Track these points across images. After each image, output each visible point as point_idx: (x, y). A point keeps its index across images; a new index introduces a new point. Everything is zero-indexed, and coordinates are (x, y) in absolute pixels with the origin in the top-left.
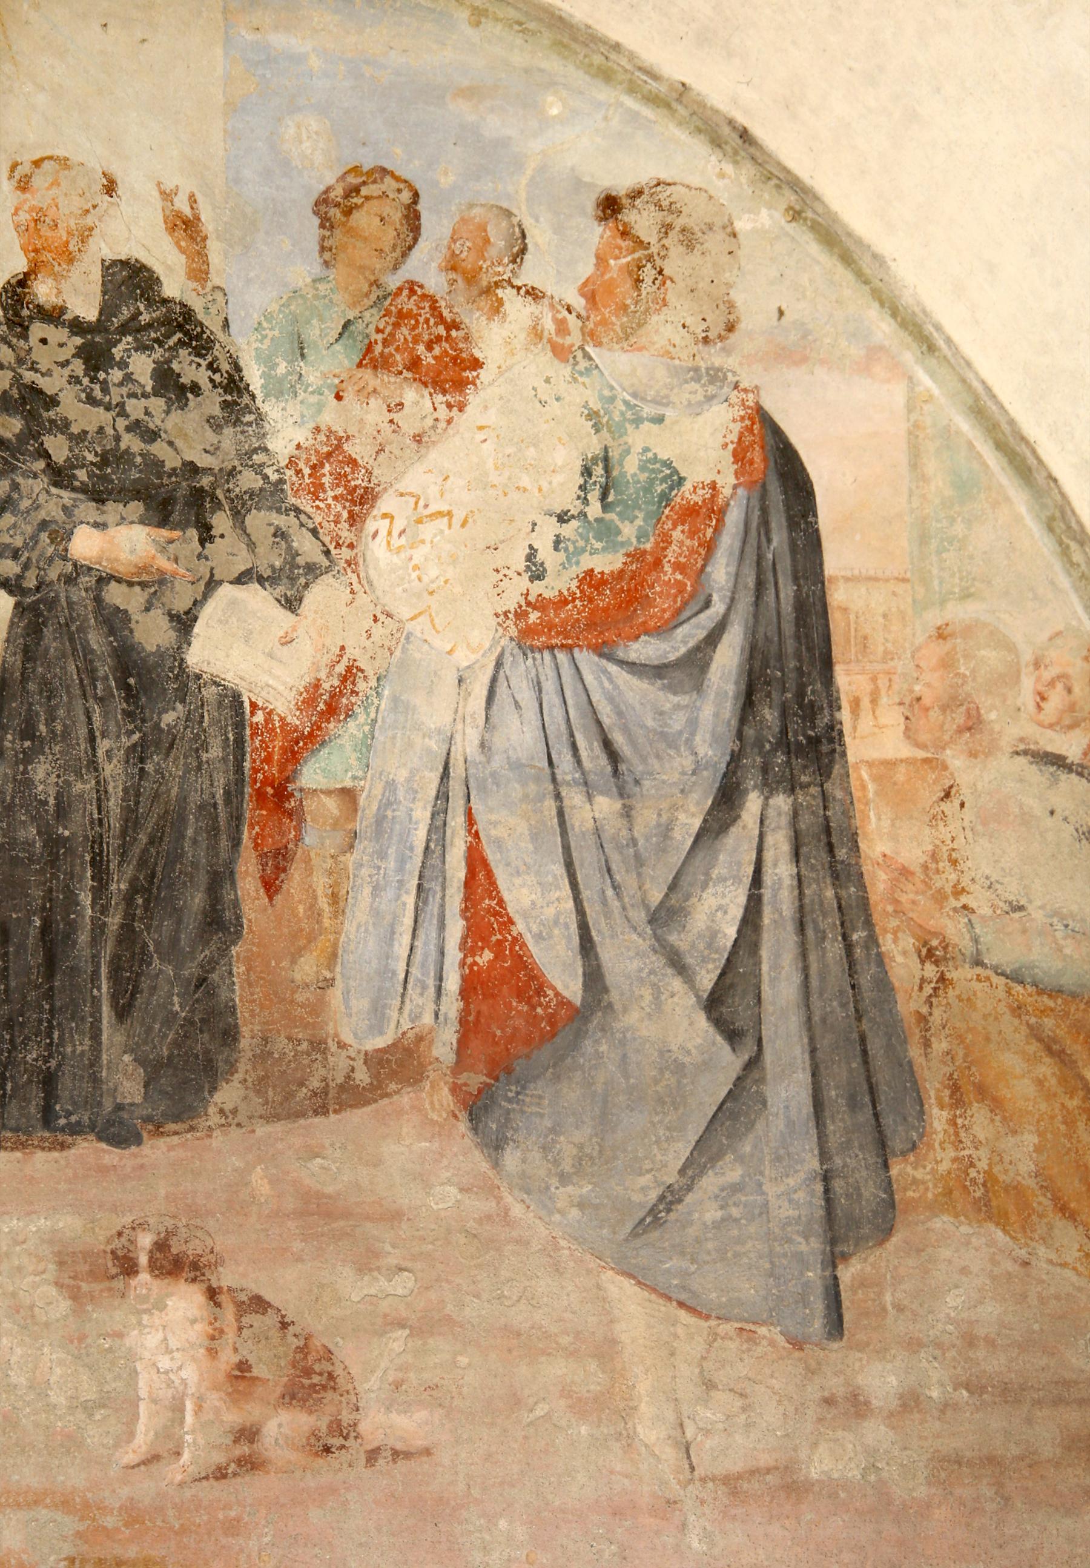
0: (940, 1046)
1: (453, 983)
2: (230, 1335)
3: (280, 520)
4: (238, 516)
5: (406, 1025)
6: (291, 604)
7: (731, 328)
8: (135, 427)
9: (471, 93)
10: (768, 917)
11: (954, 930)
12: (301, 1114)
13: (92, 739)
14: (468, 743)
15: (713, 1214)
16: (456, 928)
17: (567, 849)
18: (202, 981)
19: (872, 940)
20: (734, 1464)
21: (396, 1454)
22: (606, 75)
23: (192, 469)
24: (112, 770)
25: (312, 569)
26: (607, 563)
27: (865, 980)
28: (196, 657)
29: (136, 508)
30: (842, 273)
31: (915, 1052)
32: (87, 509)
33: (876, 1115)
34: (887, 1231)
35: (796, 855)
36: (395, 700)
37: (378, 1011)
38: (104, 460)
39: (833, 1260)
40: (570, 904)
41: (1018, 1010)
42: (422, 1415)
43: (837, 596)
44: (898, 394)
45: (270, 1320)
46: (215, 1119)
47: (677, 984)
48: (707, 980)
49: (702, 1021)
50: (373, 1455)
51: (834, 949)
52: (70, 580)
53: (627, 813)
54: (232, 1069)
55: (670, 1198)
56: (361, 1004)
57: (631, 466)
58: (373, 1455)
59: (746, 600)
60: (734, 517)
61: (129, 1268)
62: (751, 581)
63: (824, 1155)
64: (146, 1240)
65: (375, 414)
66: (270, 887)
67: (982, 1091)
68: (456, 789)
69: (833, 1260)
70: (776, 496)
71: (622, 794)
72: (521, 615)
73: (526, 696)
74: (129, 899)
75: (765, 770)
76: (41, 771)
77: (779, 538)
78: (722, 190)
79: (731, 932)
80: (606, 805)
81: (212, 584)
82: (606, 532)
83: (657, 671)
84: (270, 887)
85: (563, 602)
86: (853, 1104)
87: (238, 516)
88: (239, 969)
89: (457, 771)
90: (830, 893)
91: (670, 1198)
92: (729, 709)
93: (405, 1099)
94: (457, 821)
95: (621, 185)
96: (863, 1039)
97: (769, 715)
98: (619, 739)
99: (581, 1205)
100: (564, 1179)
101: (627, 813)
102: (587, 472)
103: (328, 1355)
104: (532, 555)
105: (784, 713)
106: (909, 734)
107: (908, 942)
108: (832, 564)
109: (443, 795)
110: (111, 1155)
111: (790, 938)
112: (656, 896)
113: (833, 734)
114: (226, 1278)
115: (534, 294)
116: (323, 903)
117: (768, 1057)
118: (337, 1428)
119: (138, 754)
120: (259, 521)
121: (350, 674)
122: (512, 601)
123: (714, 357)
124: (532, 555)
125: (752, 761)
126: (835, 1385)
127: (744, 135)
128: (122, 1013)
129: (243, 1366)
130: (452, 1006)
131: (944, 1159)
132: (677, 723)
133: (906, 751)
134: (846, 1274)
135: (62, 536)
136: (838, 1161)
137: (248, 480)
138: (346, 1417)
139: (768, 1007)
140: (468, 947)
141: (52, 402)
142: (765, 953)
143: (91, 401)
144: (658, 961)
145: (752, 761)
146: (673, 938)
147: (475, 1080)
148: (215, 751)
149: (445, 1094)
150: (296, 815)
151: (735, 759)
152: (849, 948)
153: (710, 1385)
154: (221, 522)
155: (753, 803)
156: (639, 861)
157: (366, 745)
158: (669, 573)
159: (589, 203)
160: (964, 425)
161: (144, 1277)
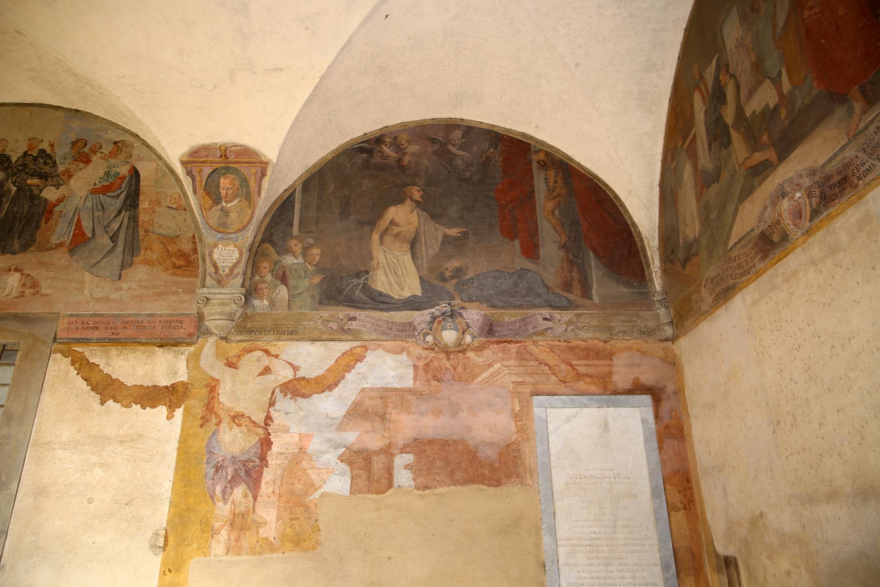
0: (145, 243)
1: (71, 235)
2: (24, 280)
3: (58, 179)
4: (52, 178)
5: (63, 240)
6: (57, 189)
7: (131, 156)
8: (39, 168)
9: (98, 130)
10: (122, 227)
11: (151, 229)
12: (43, 251)
13: (24, 205)
14: (81, 205)
15: (104, 264)
16: (73, 228)
17: (93, 219)
18: (32, 234)
19: (138, 230)
20: (99, 297)
21: (46, 295)
22: (118, 128)
23: (46, 173)
24: (26, 209)
25: (61, 185)
26: (106, 184)
27: (135, 235)
28: (42, 195)
29: (37, 177)
30: (149, 150)
31: (141, 244)
32: (30, 177)
33: (133, 252)
34: (131, 267)
35: (129, 219)
36: (71, 200)
37: (59, 238)
38: (34, 172)
39: (122, 270)
40: (92, 225)
41: (158, 238)
42: (50, 290)
43: (141, 188)
44: (155, 164)
45: (31, 277)
46: (29, 251)
47: (106, 235)
48: (111, 235)
49: (109, 240)
50: (42, 295)
51: (132, 231)
52: (25, 186)
53: (104, 214)
54: (34, 245)
55: (98, 262)
56: (56, 237)
57: (112, 172)
58: (42, 295)
59: (127, 189)
60: (127, 179)
61: (10, 270)
62: (128, 186)
63: (123, 257)
64: (14, 267)
65: (75, 166)
66: (46, 223)
67: (150, 249)
68: (77, 211)
69: (122, 270)
70: (134, 175)
71: (103, 211)
72: (92, 190)
73: (91, 200)
74: (24, 224)
75: (126, 209)
76: (15, 209)
77: (134, 181)
78: (132, 141)
79: (116, 229)
80: (100, 213)
81: (46, 186)
82: (107, 180)
83: (112, 197)
84: (46, 223)
85: (98, 188)
86: (129, 250)
87: (52, 178)
88: (38, 233)
89: (78, 208)
90: (133, 224)
91: (98, 262)
92: (122, 202)
93: (60, 249)
94: (77, 215)
95: (118, 139)
96: (133, 242)
97: (128, 202)
98: (104, 205)
99: (84, 263)
100: (82, 260)
101: (104, 214)
102: (105, 173)
103: (38, 282)
104: (95, 183)
105: (131, 202)
106: (150, 205)
107: (143, 230)
108: (142, 184)
109: (75, 212)
110: (12, 256)
111: (125, 229)
112: (106, 224)
113: (138, 205)
114: (25, 272)
115: (102, 153)
116: (54, 225)
117: (118, 244)
118: (37, 292)
119: (30, 206)
120: (55, 179)
121: (65, 197)
122: (91, 188)
123: (128, 160)
124: (95, 183)
125: (124, 208)
126: (118, 286)
127: (137, 135)
128: (18, 238)
129: (25, 283)
130: (70, 238)
131: (142, 257)
132: (114, 203)
133: (148, 207)
134: (123, 272)
135: (26, 180)
136: (125, 257)
137: (55, 174)
138: (39, 290)
139: (120, 239)
140: (75, 230)
141: (28, 165)
142: (121, 231)
143: (33, 165)
144: (104, 232)
145: (124, 208)
146: (107, 229)
147: (71, 247)
148: (42, 206)
149: (66, 249)
150: (52, 214)
151: (122, 208)
152: (134, 230)
153: (98, 286)
154: (49, 179)
155: (123, 213)
156: (104, 220)
157: (65, 206)
158: (116, 185)
159: (112, 142)
160: (164, 168)
161: (12, 272)
